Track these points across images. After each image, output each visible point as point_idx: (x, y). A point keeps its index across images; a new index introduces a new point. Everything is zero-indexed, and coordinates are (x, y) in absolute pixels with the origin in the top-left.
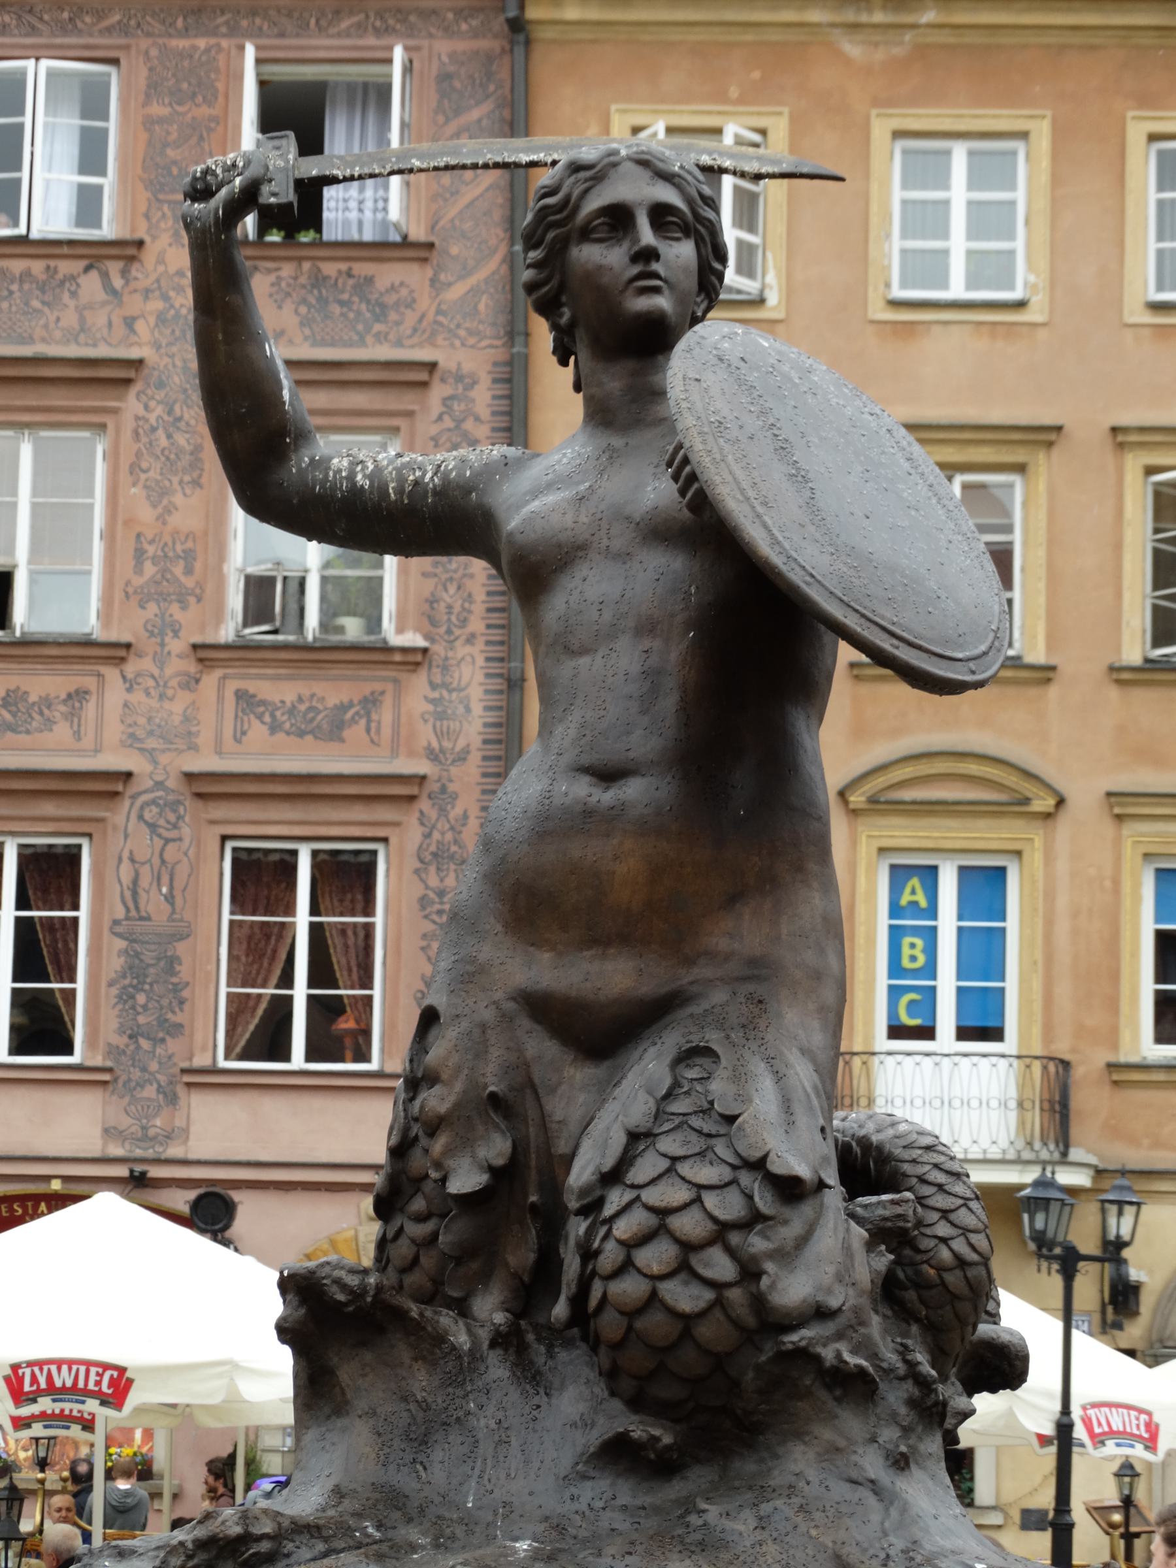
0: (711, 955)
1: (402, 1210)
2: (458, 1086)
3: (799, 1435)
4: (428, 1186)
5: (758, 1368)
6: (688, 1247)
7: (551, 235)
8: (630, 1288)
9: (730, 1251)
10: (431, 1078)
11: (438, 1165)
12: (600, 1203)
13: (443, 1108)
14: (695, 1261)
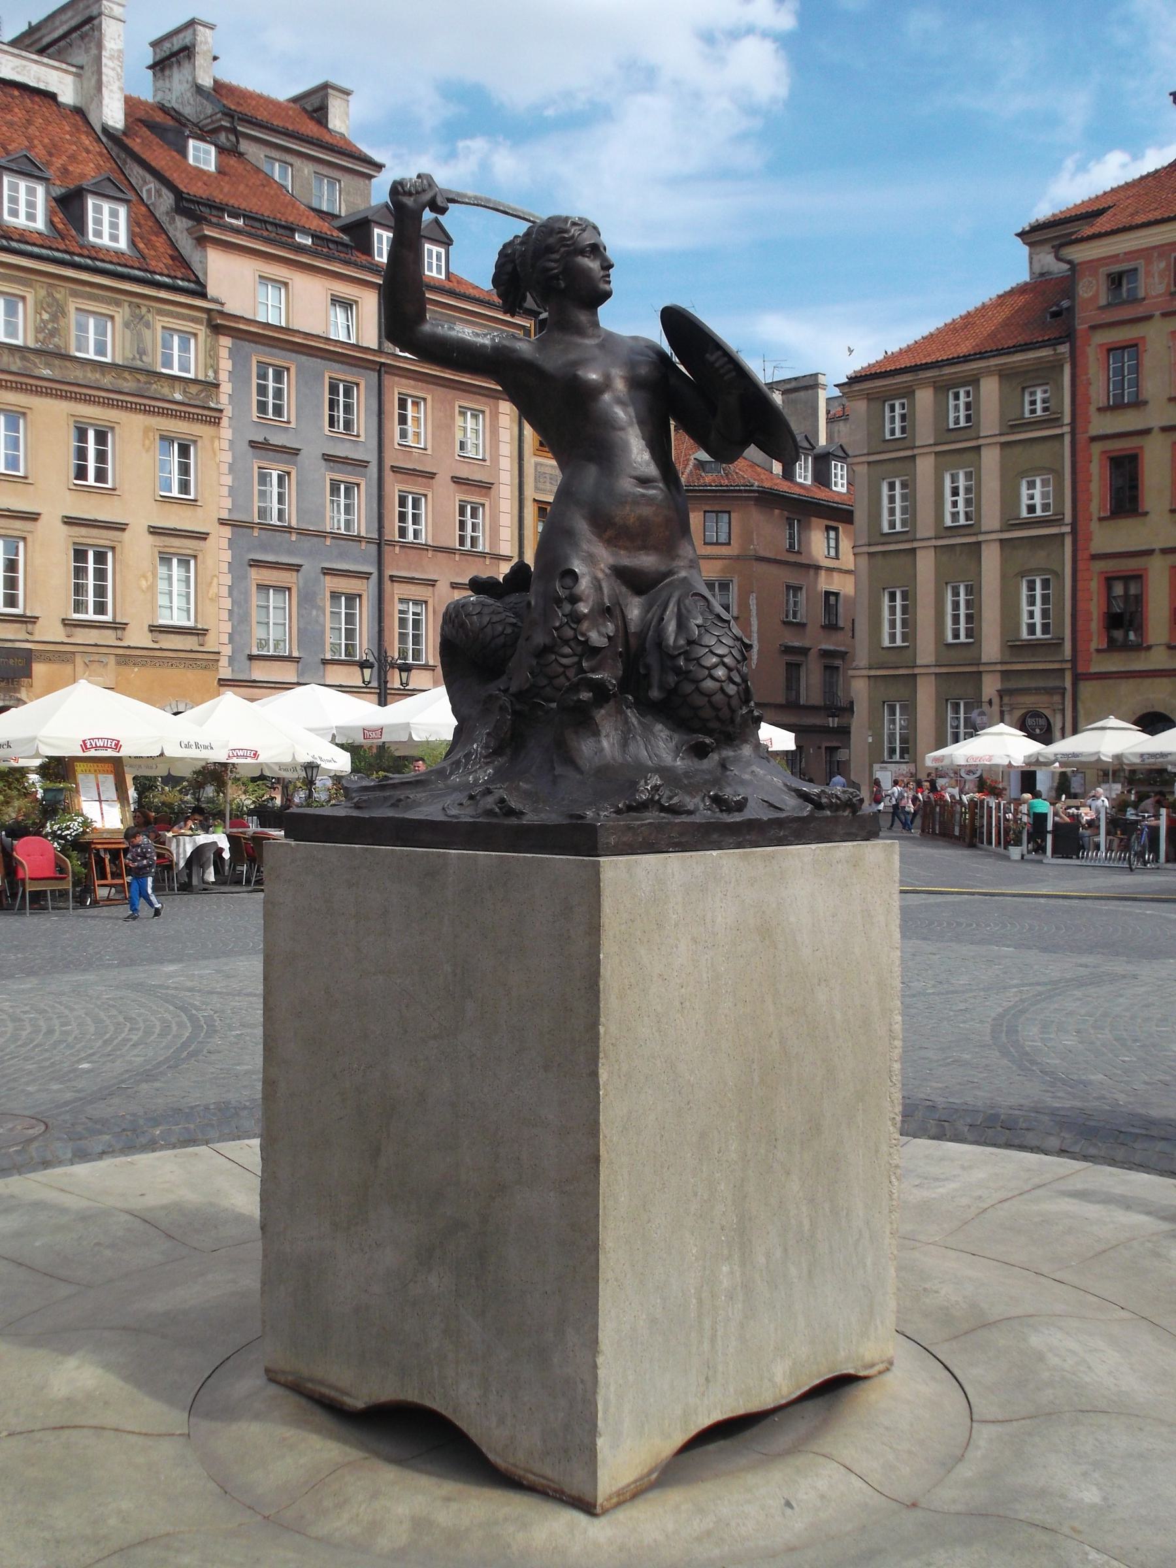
0: (678, 556)
1: (555, 653)
2: (591, 603)
3: (746, 741)
5: (742, 716)
6: (729, 669)
7: (563, 249)
8: (709, 684)
9: (738, 671)
10: (574, 599)
11: (583, 635)
13: (586, 611)
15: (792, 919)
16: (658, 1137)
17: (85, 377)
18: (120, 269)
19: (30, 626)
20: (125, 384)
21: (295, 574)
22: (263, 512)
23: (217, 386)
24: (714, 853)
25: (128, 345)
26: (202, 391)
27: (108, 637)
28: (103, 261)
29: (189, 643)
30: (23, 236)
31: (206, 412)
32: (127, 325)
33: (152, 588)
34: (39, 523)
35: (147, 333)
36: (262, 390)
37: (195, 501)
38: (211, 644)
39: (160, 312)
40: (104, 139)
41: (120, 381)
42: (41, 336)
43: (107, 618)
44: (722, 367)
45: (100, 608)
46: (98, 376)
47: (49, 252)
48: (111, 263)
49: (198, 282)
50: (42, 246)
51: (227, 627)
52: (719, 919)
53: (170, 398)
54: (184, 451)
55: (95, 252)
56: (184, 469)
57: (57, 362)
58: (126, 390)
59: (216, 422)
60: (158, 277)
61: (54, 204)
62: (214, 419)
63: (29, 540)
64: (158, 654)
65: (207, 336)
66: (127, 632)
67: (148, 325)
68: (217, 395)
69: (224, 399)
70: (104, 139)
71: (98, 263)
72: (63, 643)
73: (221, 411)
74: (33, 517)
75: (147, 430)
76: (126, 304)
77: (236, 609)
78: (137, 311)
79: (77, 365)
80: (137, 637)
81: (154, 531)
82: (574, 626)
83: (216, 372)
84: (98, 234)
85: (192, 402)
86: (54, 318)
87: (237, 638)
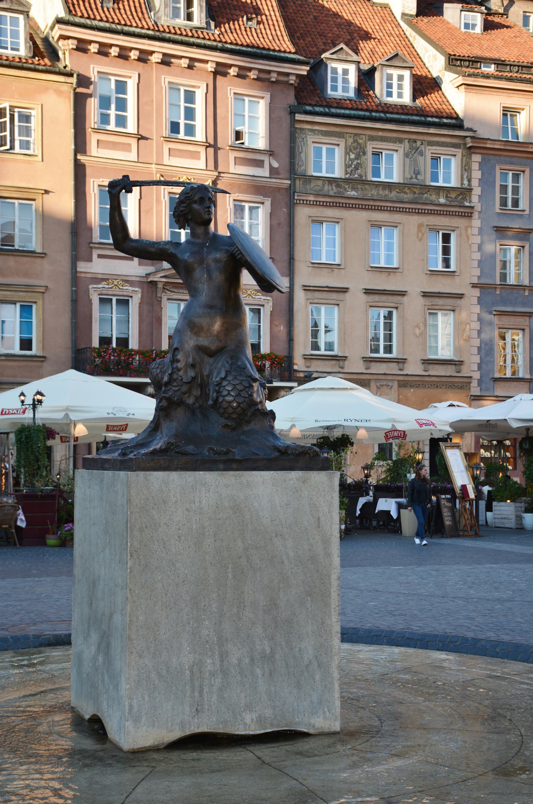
4: (178, 381)
7: (188, 202)
10: (178, 361)
12: (221, 383)
13: (182, 366)
14: (241, 393)
15: (256, 504)
16: (164, 595)
17: (378, 194)
18: (403, 117)
19: (341, 363)
20: (405, 196)
21: (527, 319)
22: (504, 277)
23: (470, 190)
24: (201, 472)
25: (407, 169)
26: (459, 195)
27: (393, 369)
28: (392, 113)
29: (450, 371)
30: (339, 103)
31: (461, 210)
32: (406, 155)
33: (423, 334)
34: (347, 294)
35: (421, 159)
36: (504, 189)
37: (454, 272)
38: (465, 372)
39: (431, 144)
40: (402, 24)
41: (402, 195)
42: (349, 170)
43: (394, 355)
44: (236, 253)
45: (388, 349)
46: (387, 192)
47: (356, 112)
48: (397, 113)
49: (457, 118)
50: (351, 109)
51: (477, 359)
52: (204, 501)
53: (436, 202)
54: (446, 238)
55: (387, 108)
56: (446, 251)
57: (359, 186)
58: (406, 200)
59: (469, 216)
60: (429, 119)
61: (362, 78)
62: (467, 214)
63: (341, 305)
64: (427, 379)
65: (463, 156)
66: (406, 365)
67: (421, 154)
68: (470, 197)
69: (475, 199)
70: (402, 24)
71: (388, 115)
72: (362, 373)
73: (473, 207)
74: (344, 290)
75: (420, 226)
76: (407, 141)
77: (483, 346)
78: (414, 145)
79: (374, 187)
80: (414, 368)
81: (426, 295)
82: (177, 372)
83: (469, 181)
84: (390, 94)
85: (452, 203)
86: (358, 157)
87: (484, 366)
